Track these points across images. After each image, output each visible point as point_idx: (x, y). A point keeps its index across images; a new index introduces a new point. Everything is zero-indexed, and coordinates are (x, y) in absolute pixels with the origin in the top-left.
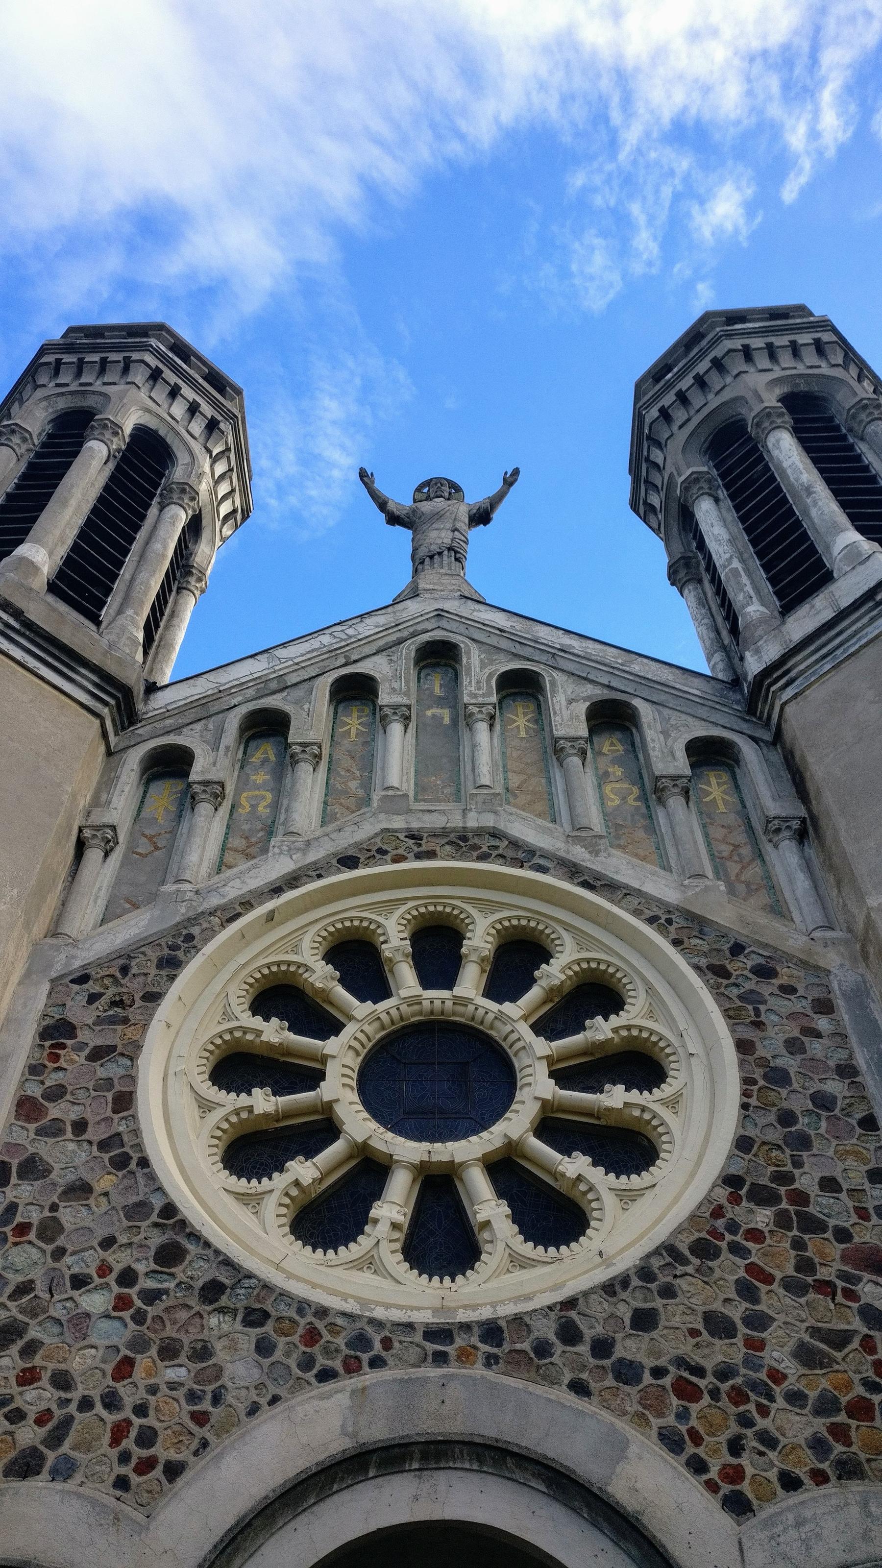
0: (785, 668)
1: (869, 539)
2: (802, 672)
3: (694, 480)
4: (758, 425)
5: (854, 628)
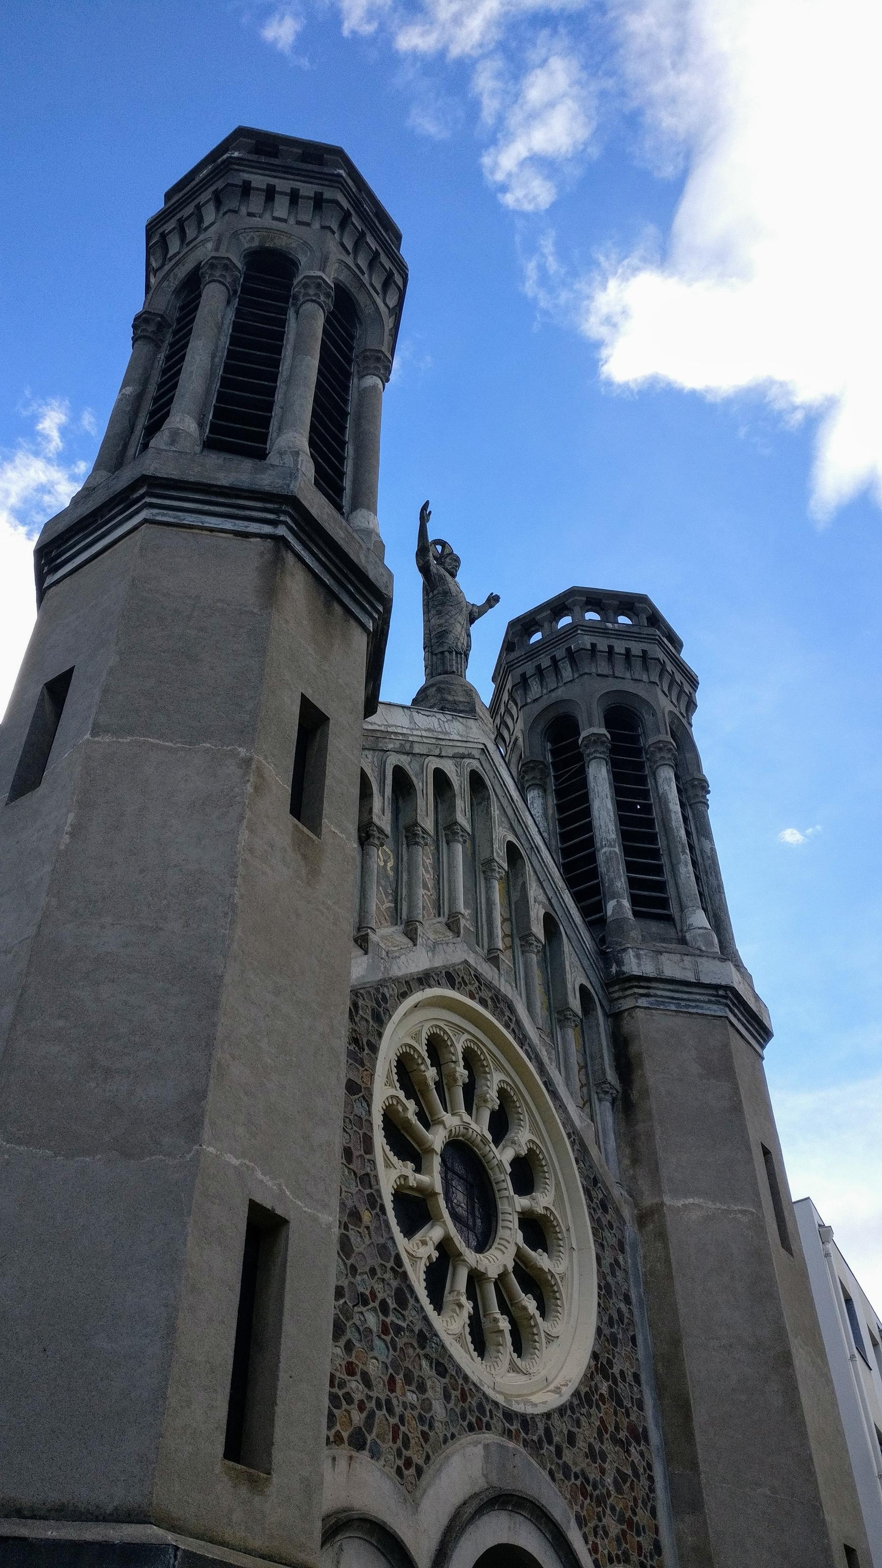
0: (649, 985)
1: (312, 456)
2: (656, 996)
3: (596, 739)
4: (306, 286)
5: (698, 997)
